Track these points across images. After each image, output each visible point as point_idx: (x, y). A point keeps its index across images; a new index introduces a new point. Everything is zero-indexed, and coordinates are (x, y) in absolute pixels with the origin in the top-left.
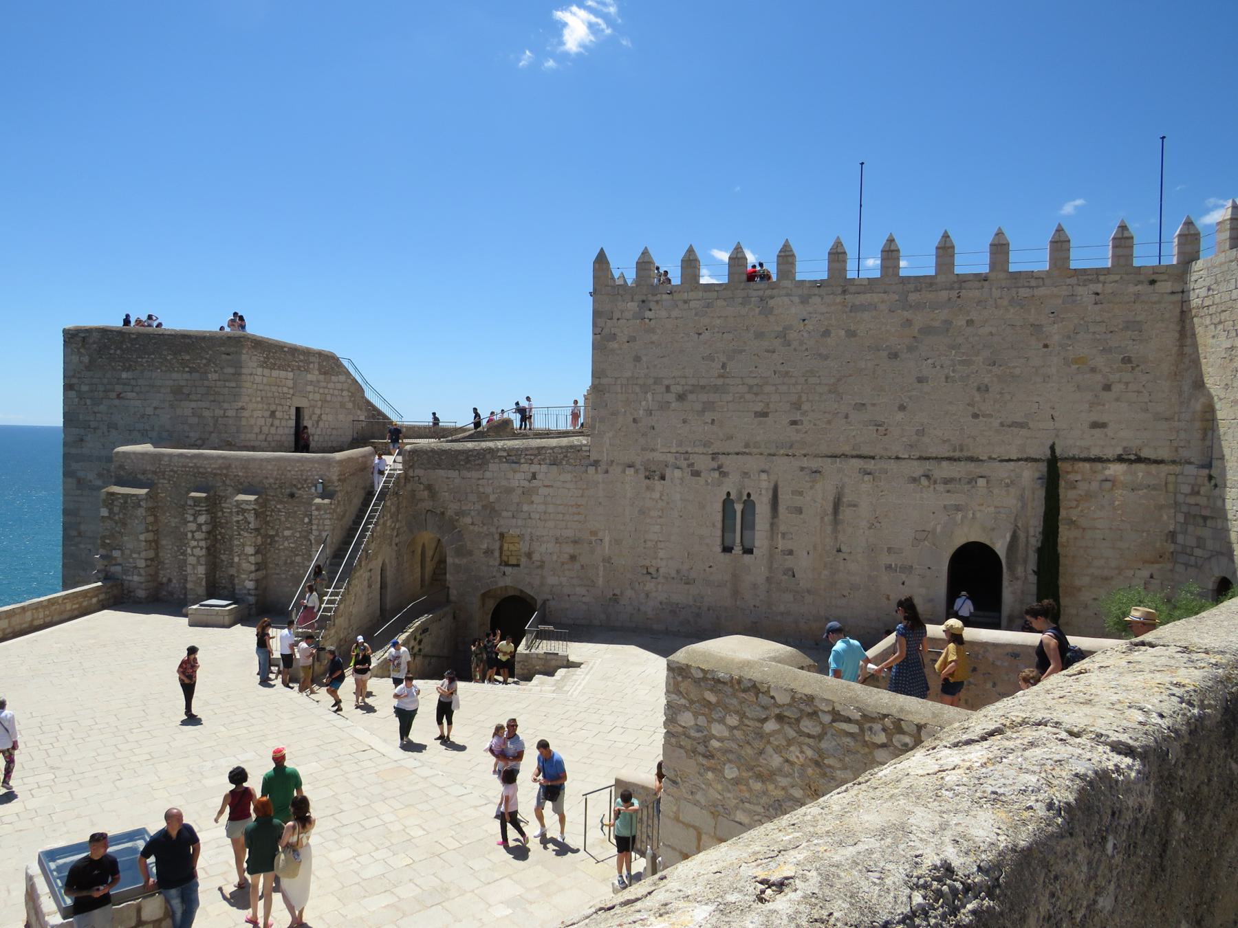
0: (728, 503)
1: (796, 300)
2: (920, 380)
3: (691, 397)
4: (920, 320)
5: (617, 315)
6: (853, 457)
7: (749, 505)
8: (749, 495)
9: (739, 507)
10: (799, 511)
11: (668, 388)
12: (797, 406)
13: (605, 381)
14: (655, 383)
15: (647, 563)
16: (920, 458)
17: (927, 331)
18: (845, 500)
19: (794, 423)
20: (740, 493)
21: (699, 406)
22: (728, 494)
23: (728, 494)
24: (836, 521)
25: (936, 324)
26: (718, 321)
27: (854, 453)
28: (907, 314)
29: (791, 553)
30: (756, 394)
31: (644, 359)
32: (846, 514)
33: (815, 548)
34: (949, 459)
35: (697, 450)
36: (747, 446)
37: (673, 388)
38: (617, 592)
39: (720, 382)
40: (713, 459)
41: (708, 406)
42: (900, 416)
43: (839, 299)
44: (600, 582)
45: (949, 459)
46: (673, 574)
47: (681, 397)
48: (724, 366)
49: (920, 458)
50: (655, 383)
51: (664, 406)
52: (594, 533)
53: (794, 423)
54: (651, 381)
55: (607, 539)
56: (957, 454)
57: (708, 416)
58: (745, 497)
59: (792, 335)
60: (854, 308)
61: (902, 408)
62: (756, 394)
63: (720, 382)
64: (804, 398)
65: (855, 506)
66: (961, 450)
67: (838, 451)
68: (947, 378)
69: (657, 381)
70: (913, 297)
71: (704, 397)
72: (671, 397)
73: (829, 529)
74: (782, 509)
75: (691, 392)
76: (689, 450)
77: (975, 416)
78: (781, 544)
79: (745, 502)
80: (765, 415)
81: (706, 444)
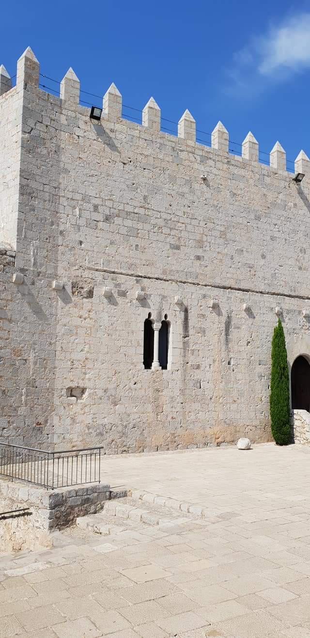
0: (148, 324)
1: (198, 158)
2: (273, 238)
3: (118, 221)
4: (271, 197)
5: (46, 121)
6: (236, 289)
7: (165, 325)
8: (166, 316)
9: (157, 326)
10: (203, 331)
11: (96, 207)
12: (200, 244)
13: (33, 185)
14: (83, 200)
15: (73, 385)
16: (274, 294)
17: (274, 204)
18: (232, 323)
19: (198, 258)
20: (160, 314)
21: (124, 231)
22: (150, 315)
23: (150, 315)
24: (227, 341)
25: (279, 201)
26: (140, 158)
27: (237, 287)
28: (265, 191)
29: (198, 367)
30: (171, 229)
31: (72, 173)
32: (234, 334)
33: (214, 361)
34: (289, 296)
35: (124, 272)
36: (164, 272)
37: (100, 209)
38: (41, 420)
39: (142, 211)
40: (137, 281)
41: (134, 233)
42: (262, 262)
43: (226, 166)
44: (22, 411)
45: (289, 296)
46: (100, 393)
47: (107, 219)
48: (145, 198)
49: (274, 294)
50: (83, 200)
51: (93, 224)
52: (17, 352)
53: (198, 258)
54: (78, 197)
55: (32, 358)
56: (293, 294)
57: (133, 241)
58: (163, 319)
59: (196, 186)
60: (234, 177)
61: (263, 257)
62: (171, 229)
63: (142, 211)
64: (205, 238)
65: (239, 328)
66: (295, 291)
67: (227, 284)
68: (286, 240)
69: (85, 198)
70: (268, 180)
71: (128, 223)
72: (100, 217)
73: (224, 348)
74: (191, 331)
75: (118, 216)
76: (116, 270)
77: (300, 268)
78: (192, 360)
79: (163, 322)
80: (178, 248)
81: (131, 266)
